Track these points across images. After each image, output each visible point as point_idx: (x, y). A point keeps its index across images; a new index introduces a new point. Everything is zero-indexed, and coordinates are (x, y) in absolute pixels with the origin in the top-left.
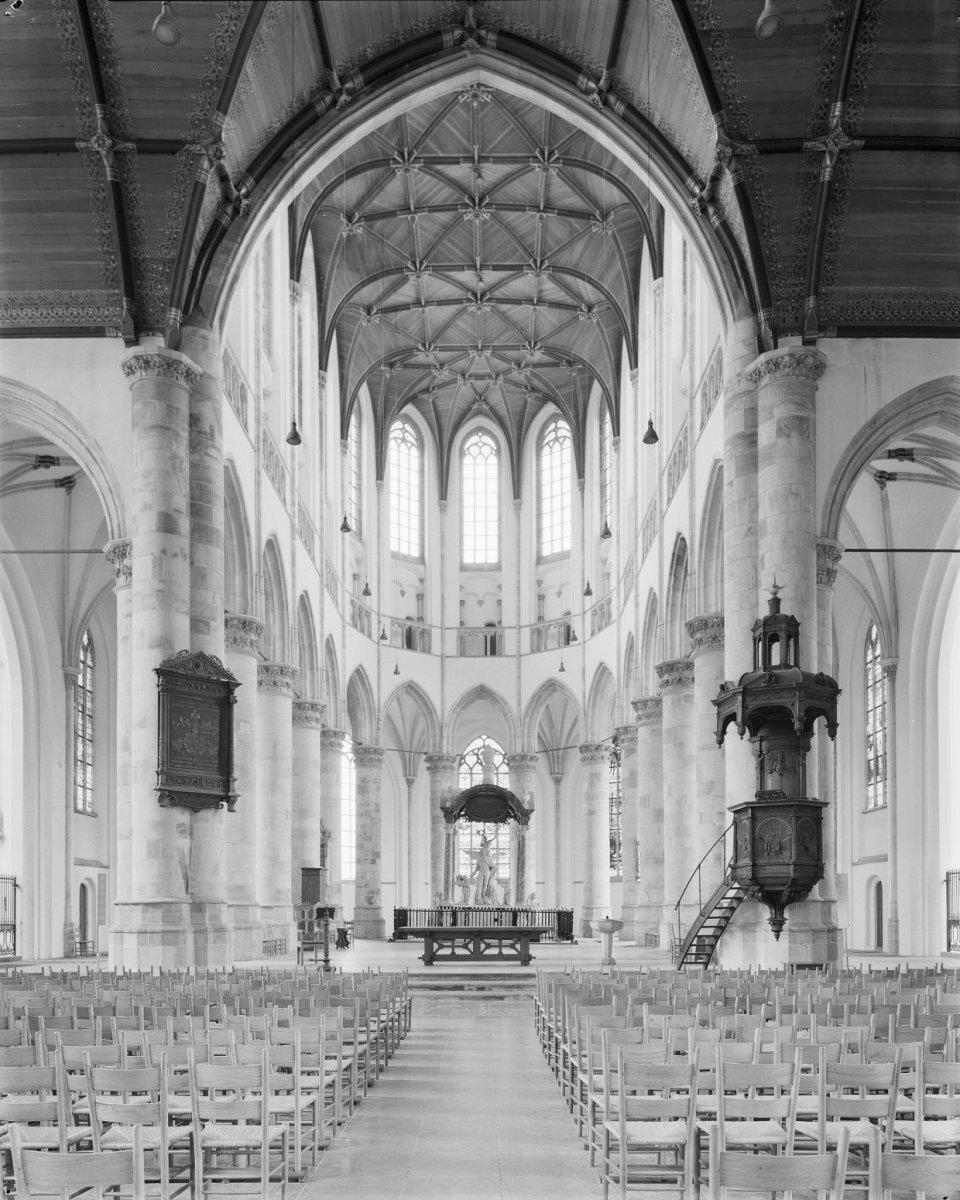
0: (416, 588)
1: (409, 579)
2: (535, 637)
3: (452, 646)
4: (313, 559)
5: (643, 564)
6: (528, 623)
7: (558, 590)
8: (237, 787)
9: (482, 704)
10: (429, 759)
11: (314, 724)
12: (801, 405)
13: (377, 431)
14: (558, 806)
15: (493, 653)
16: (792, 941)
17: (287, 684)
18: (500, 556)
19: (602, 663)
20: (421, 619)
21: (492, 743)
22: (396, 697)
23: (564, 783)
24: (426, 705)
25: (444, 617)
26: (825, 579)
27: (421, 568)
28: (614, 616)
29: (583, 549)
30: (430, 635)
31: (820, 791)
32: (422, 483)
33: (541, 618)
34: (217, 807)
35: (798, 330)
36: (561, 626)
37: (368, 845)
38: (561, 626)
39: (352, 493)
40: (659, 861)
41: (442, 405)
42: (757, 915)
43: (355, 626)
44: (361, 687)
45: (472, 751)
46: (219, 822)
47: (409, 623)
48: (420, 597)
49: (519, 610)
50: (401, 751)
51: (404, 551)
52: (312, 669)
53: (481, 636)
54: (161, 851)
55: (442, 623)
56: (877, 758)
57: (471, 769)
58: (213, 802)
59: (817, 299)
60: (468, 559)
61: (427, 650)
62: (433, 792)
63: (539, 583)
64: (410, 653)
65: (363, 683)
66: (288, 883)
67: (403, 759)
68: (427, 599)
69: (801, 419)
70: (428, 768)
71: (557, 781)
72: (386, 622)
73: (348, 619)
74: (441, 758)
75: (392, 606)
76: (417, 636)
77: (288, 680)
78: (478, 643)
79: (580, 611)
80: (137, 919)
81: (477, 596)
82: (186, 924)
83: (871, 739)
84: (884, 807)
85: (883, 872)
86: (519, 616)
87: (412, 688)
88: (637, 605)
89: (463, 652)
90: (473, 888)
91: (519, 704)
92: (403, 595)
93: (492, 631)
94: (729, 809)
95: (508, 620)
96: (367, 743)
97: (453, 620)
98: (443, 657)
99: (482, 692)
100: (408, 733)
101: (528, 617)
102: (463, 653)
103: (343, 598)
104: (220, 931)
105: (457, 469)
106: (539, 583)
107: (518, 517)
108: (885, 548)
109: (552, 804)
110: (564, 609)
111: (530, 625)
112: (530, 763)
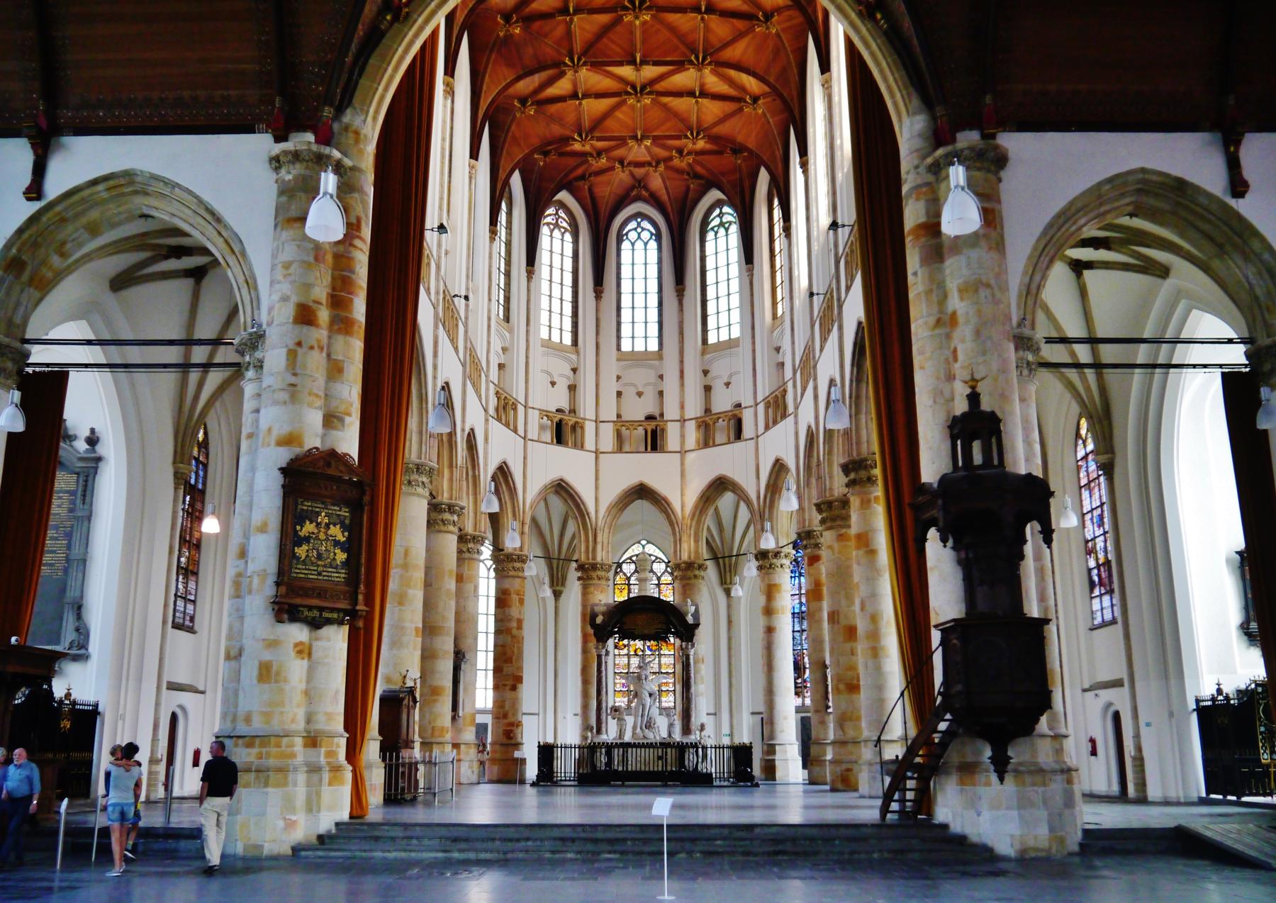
0: (568, 378)
1: (561, 369)
2: (702, 428)
3: (608, 441)
4: (456, 349)
5: (821, 350)
6: (694, 416)
7: (726, 381)
9: (642, 506)
10: (581, 567)
11: (451, 528)
15: (654, 448)
17: (423, 483)
19: (777, 461)
20: (573, 411)
21: (651, 549)
22: (543, 497)
24: (578, 506)
27: (574, 357)
28: (791, 409)
29: (753, 337)
30: (582, 428)
31: (1039, 606)
33: (708, 411)
36: (730, 420)
38: (730, 420)
40: (853, 688)
42: (979, 753)
43: (499, 419)
44: (503, 485)
45: (630, 558)
52: (451, 466)
53: (641, 431)
55: (597, 416)
56: (1098, 566)
57: (628, 579)
61: (579, 445)
62: (584, 606)
63: (706, 373)
68: (580, 390)
70: (579, 579)
72: (534, 416)
73: (492, 411)
74: (594, 567)
76: (567, 431)
77: (425, 479)
79: (752, 403)
81: (635, 385)
83: (1090, 544)
84: (1113, 621)
85: (1119, 699)
86: (682, 407)
87: (561, 488)
88: (816, 397)
89: (620, 448)
92: (553, 387)
93: (652, 425)
94: (936, 626)
95: (671, 412)
97: (609, 413)
98: (597, 452)
99: (642, 492)
101: (694, 408)
102: (620, 448)
103: (487, 389)
106: (706, 373)
110: (736, 400)
112: (697, 572)
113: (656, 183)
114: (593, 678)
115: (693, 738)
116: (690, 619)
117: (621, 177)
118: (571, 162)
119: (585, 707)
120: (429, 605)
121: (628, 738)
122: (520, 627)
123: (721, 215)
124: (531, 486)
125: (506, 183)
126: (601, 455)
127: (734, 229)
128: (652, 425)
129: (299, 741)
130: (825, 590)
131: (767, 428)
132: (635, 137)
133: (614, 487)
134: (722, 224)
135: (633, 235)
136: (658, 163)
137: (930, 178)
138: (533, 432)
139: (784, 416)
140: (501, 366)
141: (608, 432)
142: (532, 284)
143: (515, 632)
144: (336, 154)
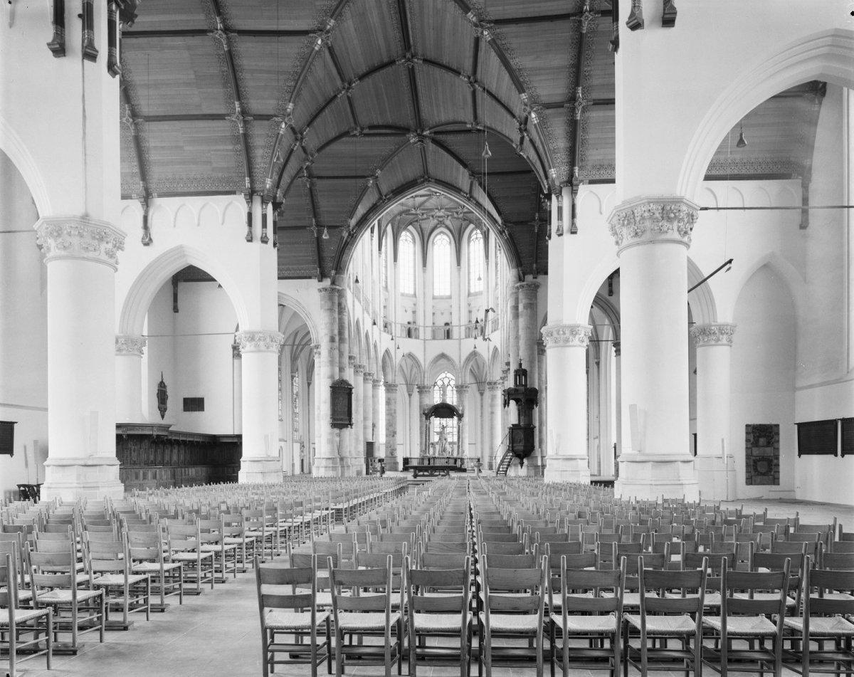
1: (409, 304)
2: (467, 330)
3: (429, 335)
8: (353, 421)
9: (443, 361)
10: (419, 388)
12: (531, 299)
13: (394, 237)
14: (482, 406)
16: (528, 469)
18: (451, 292)
20: (414, 322)
21: (449, 375)
23: (484, 395)
25: (424, 323)
26: (541, 352)
27: (414, 299)
32: (415, 259)
34: (347, 427)
35: (531, 273)
37: (391, 429)
39: (383, 270)
41: (423, 226)
43: (385, 331)
46: (347, 431)
47: (409, 326)
48: (414, 312)
49: (460, 317)
50: (407, 384)
51: (406, 292)
54: (331, 442)
58: (345, 426)
59: (537, 265)
60: (436, 294)
61: (417, 338)
62: (421, 402)
63: (469, 305)
64: (410, 339)
65: (389, 356)
66: (362, 448)
67: (407, 387)
69: (531, 304)
71: (482, 394)
74: (424, 387)
75: (402, 318)
76: (413, 332)
78: (441, 333)
80: (324, 463)
82: (338, 465)
87: (410, 356)
90: (437, 447)
91: (460, 362)
93: (447, 327)
95: (455, 322)
96: (390, 382)
98: (425, 340)
99: (443, 356)
100: (409, 371)
101: (464, 321)
102: (434, 338)
104: (348, 467)
105: (431, 249)
106: (469, 305)
107: (459, 274)
108: (742, 206)
109: (479, 406)
111: (465, 325)
113: (448, 222)
114: (426, 432)
115: (460, 456)
116: (460, 412)
117: (433, 222)
118: (411, 217)
119: (421, 443)
120: (365, 411)
121: (437, 455)
122: (395, 413)
123: (476, 234)
124: (397, 358)
125: (385, 231)
126: (427, 341)
127: (482, 241)
128: (447, 327)
129: (338, 459)
130: (517, 397)
131: (492, 332)
132: (437, 209)
133: (432, 354)
134: (477, 238)
135: (439, 242)
136: (448, 216)
137: (517, 290)
138: (398, 335)
139: (497, 329)
140: (385, 307)
141: (429, 331)
142: (396, 270)
143: (393, 414)
144: (337, 287)
